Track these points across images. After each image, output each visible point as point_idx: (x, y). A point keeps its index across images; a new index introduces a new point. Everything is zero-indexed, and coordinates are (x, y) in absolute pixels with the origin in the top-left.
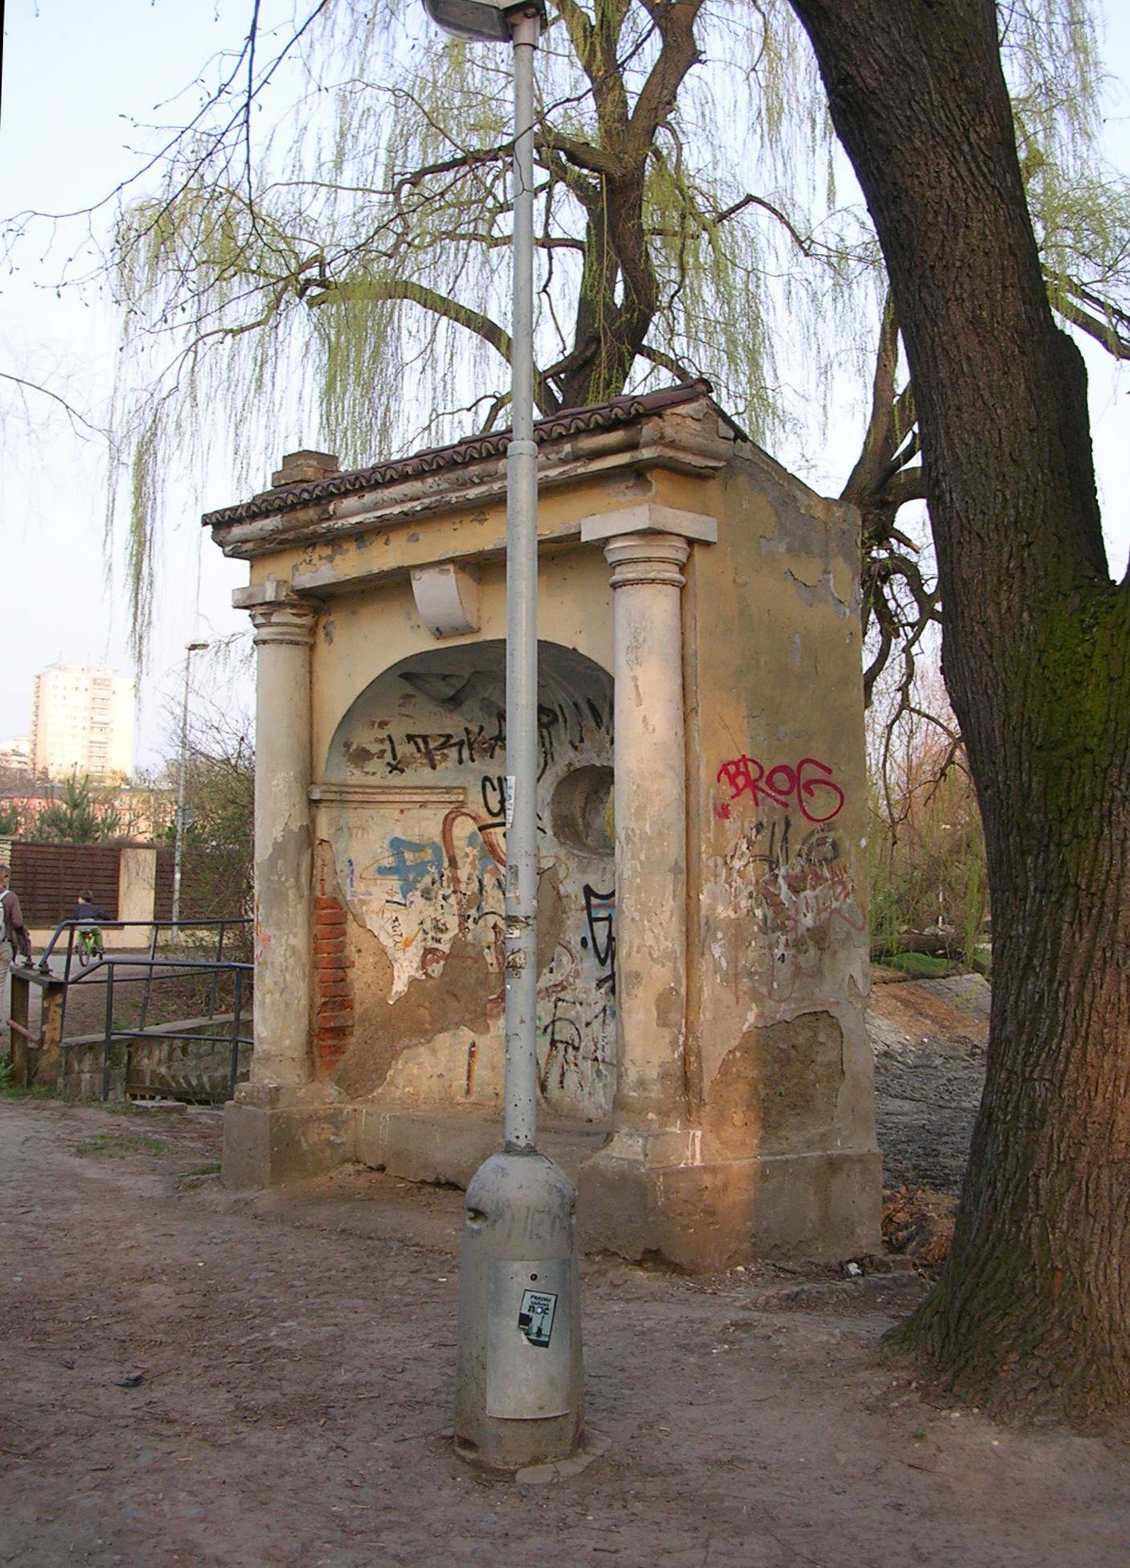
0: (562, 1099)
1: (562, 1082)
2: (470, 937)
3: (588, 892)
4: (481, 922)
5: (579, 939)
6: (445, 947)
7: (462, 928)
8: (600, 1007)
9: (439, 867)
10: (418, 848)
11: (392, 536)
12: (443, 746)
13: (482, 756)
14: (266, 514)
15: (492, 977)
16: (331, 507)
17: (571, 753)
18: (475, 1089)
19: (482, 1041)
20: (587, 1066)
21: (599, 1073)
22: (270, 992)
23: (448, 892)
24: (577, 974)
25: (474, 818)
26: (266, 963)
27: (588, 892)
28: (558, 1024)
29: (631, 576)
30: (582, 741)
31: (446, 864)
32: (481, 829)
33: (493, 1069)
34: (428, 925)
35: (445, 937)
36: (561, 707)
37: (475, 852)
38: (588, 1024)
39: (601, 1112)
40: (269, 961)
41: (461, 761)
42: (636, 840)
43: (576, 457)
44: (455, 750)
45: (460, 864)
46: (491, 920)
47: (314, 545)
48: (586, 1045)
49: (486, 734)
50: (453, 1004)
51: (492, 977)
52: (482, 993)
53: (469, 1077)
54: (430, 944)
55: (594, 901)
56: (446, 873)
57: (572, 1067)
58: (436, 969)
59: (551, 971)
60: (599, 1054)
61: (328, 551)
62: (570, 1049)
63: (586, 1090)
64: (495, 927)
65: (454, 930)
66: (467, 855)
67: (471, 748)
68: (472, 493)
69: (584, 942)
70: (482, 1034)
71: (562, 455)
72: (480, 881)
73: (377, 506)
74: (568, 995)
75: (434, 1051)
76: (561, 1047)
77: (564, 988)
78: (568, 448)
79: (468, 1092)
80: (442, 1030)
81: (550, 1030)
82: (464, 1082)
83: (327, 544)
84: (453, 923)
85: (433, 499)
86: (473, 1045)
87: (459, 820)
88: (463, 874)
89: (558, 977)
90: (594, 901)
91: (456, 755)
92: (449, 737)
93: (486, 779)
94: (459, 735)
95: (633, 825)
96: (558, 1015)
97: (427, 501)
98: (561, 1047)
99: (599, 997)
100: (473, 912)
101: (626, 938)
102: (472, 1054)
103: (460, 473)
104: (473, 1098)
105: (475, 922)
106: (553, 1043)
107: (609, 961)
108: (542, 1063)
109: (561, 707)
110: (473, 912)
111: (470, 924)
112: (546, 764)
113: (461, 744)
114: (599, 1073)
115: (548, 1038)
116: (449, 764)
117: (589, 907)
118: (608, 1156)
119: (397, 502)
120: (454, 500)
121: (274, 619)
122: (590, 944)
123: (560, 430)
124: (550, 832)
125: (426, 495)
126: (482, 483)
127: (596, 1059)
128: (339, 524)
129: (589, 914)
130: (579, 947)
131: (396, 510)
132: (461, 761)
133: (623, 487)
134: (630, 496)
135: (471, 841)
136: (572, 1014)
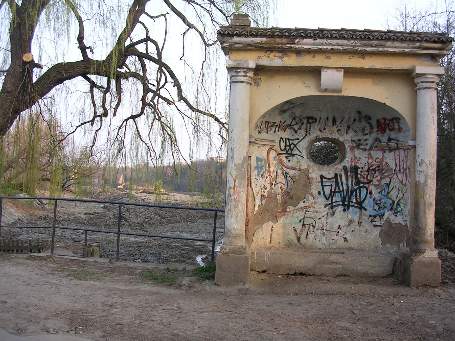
0: (306, 243)
1: (307, 237)
2: (273, 191)
3: (322, 177)
4: (276, 186)
5: (317, 192)
6: (266, 194)
7: (271, 188)
8: (325, 213)
9: (266, 167)
10: (261, 160)
11: (316, 55)
12: (272, 126)
13: (281, 130)
14: (261, 36)
15: (279, 204)
16: (297, 40)
17: (319, 133)
18: (272, 242)
19: (275, 226)
20: (319, 232)
21: (324, 234)
22: (240, 211)
23: (267, 175)
24: (315, 203)
25: (276, 151)
26: (239, 201)
27: (322, 177)
28: (306, 219)
29: (427, 86)
30: (325, 129)
31: (267, 166)
32: (278, 154)
33: (278, 234)
34: (262, 187)
35: (266, 191)
36: (320, 118)
37: (276, 162)
38: (319, 219)
39: (324, 246)
40: (240, 200)
41: (275, 132)
42: (432, 164)
43: (419, 48)
44: (275, 127)
45: (271, 166)
46: (280, 185)
47: (272, 51)
48: (319, 225)
49: (286, 124)
50: (267, 213)
51: (279, 204)
52: (276, 210)
53: (271, 238)
54: (263, 193)
55: (324, 180)
56: (267, 169)
57: (312, 232)
58: (264, 201)
59: (304, 202)
60: (324, 228)
61: (280, 55)
62: (311, 227)
63: (318, 240)
64: (281, 187)
65: (268, 189)
66: (273, 163)
67: (279, 128)
68: (368, 49)
69: (319, 193)
70: (275, 223)
71: (415, 46)
72: (277, 172)
73: (321, 44)
74: (311, 210)
75: (262, 230)
76: (307, 226)
77: (309, 207)
78: (418, 44)
79: (270, 243)
80: (264, 222)
81: (302, 221)
82: (269, 240)
83: (279, 52)
84: (268, 186)
85: (349, 47)
86: (272, 227)
87: (271, 151)
88: (272, 170)
89: (307, 204)
90: (324, 180)
91: (274, 130)
92: (275, 123)
93: (281, 138)
94: (278, 123)
95: (432, 160)
96: (306, 216)
97: (346, 48)
98: (307, 226)
99: (326, 210)
100: (274, 183)
101: (428, 193)
102: (272, 230)
103: (367, 42)
104: (272, 245)
105: (275, 186)
106: (304, 225)
107: (330, 199)
108: (298, 231)
109: (320, 118)
110: (274, 183)
111: (273, 186)
112: (306, 135)
113: (277, 126)
114: (324, 234)
115: (301, 223)
116: (271, 132)
117: (322, 182)
118: (424, 257)
119: (331, 45)
120: (359, 50)
121: (248, 74)
122: (322, 193)
123: (419, 38)
124: (305, 157)
125: (347, 45)
126: (376, 47)
127: (323, 229)
128: (297, 46)
129: (322, 184)
130: (317, 194)
131: (329, 47)
132: (275, 132)
133: (426, 59)
134: (429, 63)
135: (275, 158)
136: (313, 215)
